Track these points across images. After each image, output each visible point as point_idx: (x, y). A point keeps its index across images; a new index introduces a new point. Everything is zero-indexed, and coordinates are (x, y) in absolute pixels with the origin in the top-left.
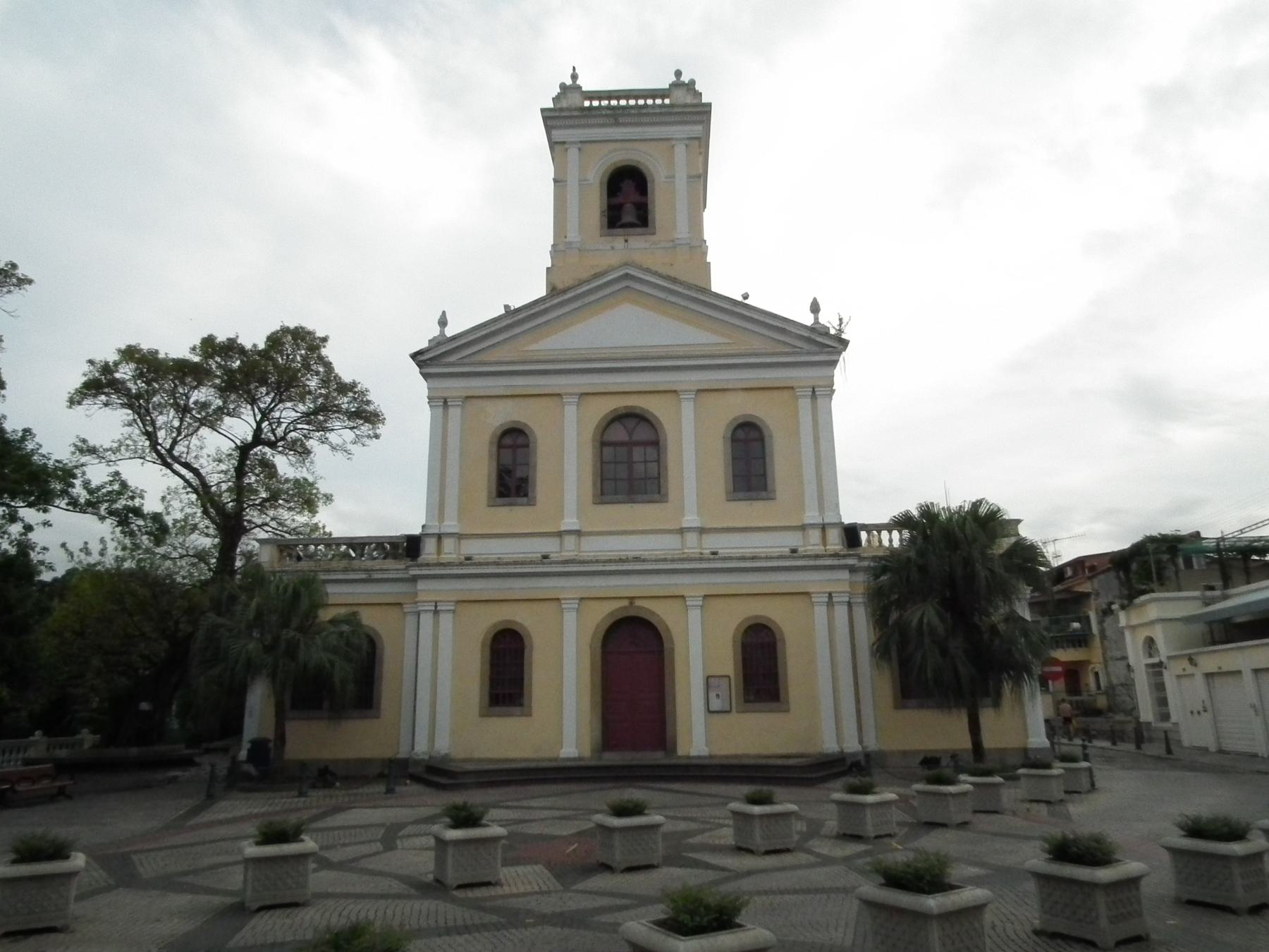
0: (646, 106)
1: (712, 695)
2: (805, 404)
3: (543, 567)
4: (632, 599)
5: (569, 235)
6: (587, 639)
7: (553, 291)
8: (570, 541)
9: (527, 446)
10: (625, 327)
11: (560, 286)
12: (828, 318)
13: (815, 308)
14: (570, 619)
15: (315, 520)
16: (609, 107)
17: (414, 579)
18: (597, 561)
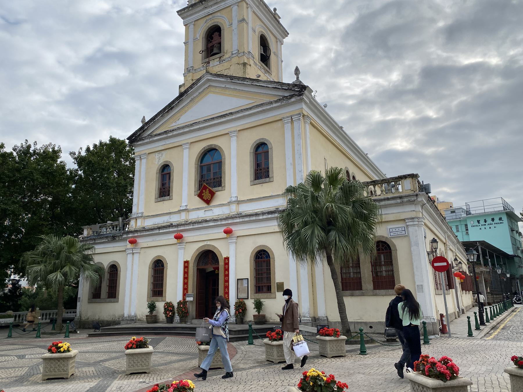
7: (181, 95)
13: (297, 71)
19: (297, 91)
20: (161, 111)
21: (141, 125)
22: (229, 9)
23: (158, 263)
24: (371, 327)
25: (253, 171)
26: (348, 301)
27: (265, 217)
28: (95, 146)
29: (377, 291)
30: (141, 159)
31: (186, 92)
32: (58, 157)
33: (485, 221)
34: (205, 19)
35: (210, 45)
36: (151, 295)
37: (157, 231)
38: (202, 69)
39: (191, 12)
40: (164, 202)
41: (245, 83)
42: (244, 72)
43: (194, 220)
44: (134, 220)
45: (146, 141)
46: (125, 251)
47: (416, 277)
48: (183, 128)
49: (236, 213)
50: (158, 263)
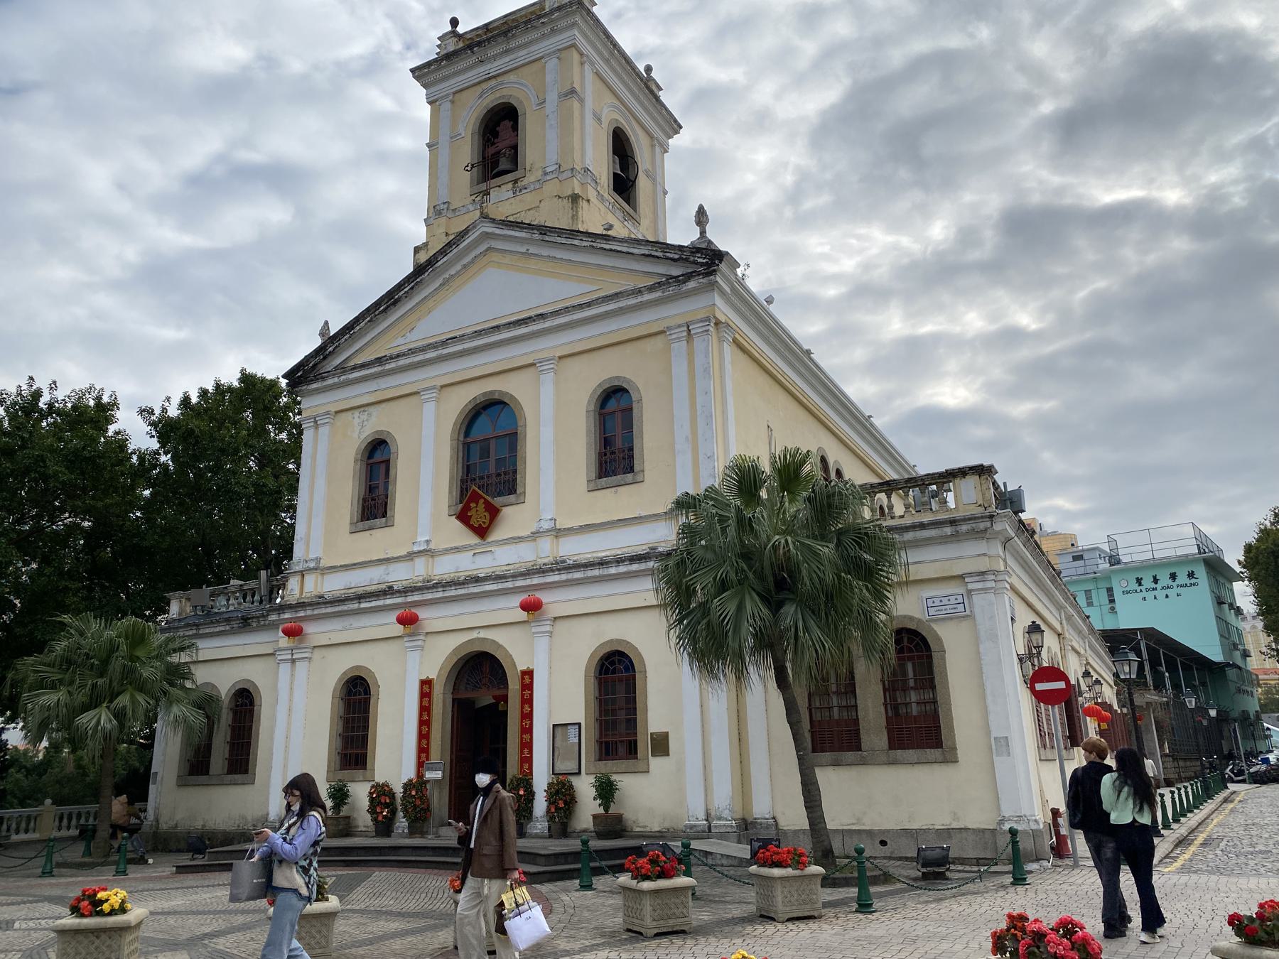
2: (680, 347)
7: (419, 270)
13: (701, 217)
19: (702, 264)
20: (368, 310)
21: (318, 342)
22: (536, 66)
23: (355, 686)
24: (883, 843)
25: (594, 457)
26: (826, 777)
27: (622, 569)
28: (204, 393)
29: (899, 752)
30: (316, 426)
31: (431, 262)
32: (110, 420)
33: (1156, 581)
34: (479, 89)
35: (491, 150)
36: (338, 766)
37: (354, 605)
38: (471, 208)
39: (445, 72)
41: (576, 242)
42: (574, 217)
43: (447, 578)
44: (298, 578)
45: (330, 381)
46: (273, 654)
47: (991, 718)
48: (423, 349)
49: (551, 559)
50: (355, 686)
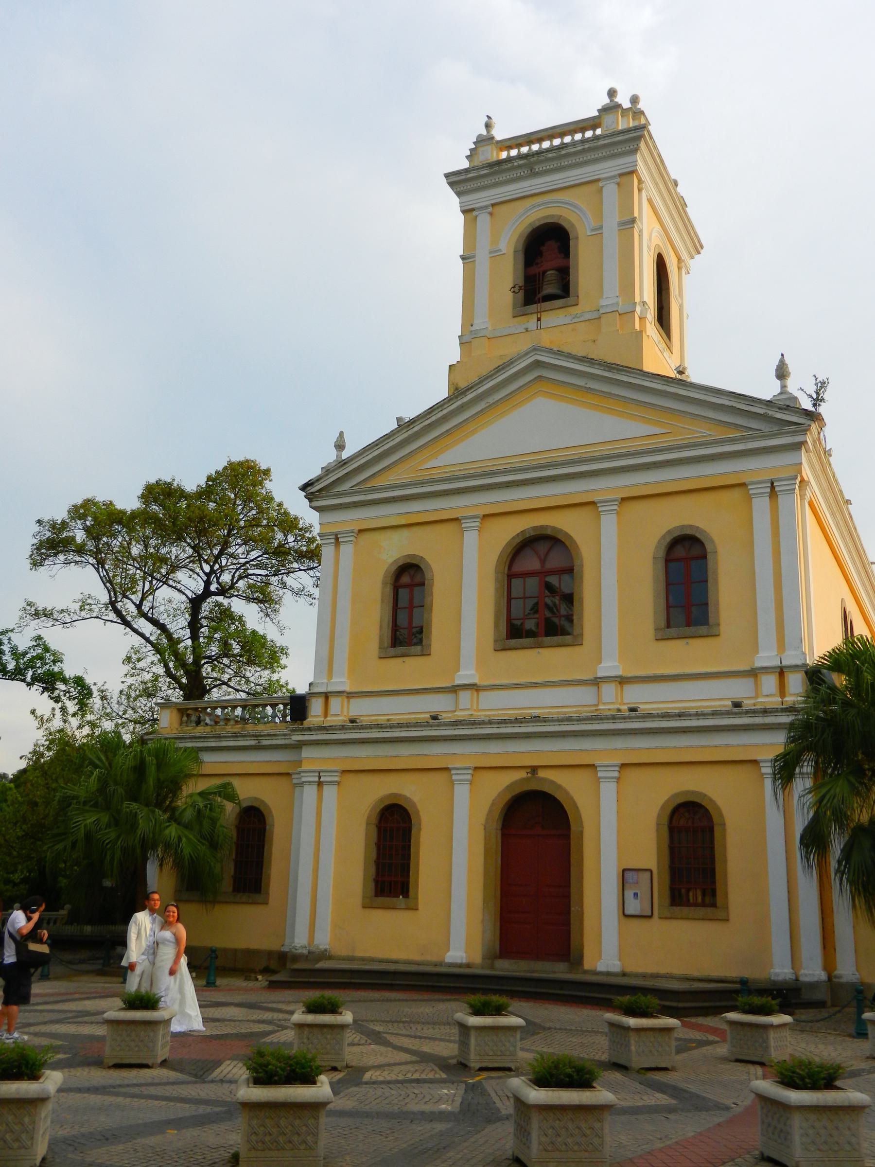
0: (563, 146)
1: (629, 894)
2: (761, 505)
3: (434, 730)
4: (534, 769)
5: (475, 322)
6: (481, 817)
7: (456, 392)
8: (465, 697)
9: (423, 584)
10: (541, 426)
11: (463, 385)
12: (800, 387)
13: (782, 373)
14: (462, 793)
15: (275, 677)
16: (520, 157)
17: (299, 746)
18: (490, 722)
22: (593, 188)
36: (373, 893)
40: (407, 660)
